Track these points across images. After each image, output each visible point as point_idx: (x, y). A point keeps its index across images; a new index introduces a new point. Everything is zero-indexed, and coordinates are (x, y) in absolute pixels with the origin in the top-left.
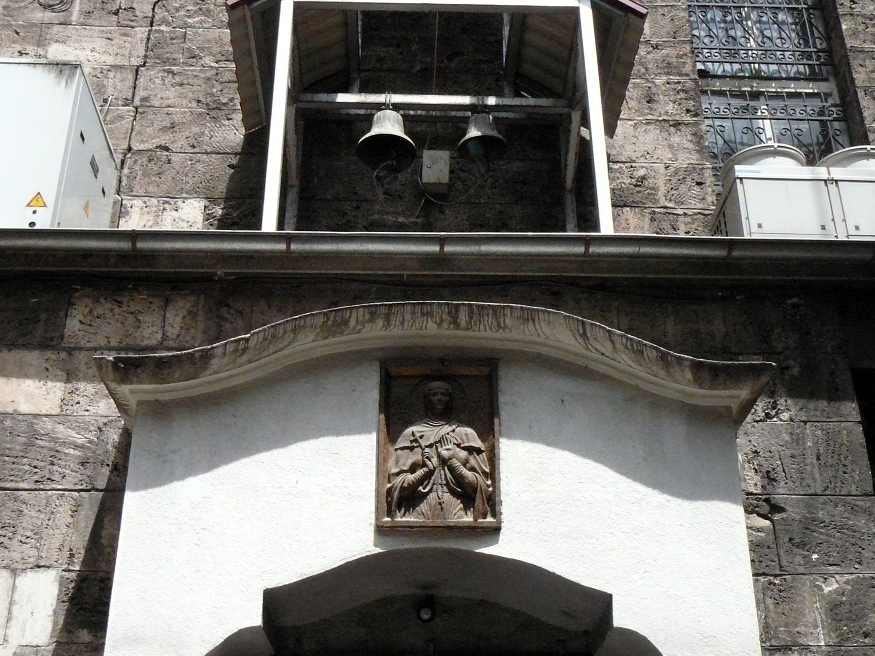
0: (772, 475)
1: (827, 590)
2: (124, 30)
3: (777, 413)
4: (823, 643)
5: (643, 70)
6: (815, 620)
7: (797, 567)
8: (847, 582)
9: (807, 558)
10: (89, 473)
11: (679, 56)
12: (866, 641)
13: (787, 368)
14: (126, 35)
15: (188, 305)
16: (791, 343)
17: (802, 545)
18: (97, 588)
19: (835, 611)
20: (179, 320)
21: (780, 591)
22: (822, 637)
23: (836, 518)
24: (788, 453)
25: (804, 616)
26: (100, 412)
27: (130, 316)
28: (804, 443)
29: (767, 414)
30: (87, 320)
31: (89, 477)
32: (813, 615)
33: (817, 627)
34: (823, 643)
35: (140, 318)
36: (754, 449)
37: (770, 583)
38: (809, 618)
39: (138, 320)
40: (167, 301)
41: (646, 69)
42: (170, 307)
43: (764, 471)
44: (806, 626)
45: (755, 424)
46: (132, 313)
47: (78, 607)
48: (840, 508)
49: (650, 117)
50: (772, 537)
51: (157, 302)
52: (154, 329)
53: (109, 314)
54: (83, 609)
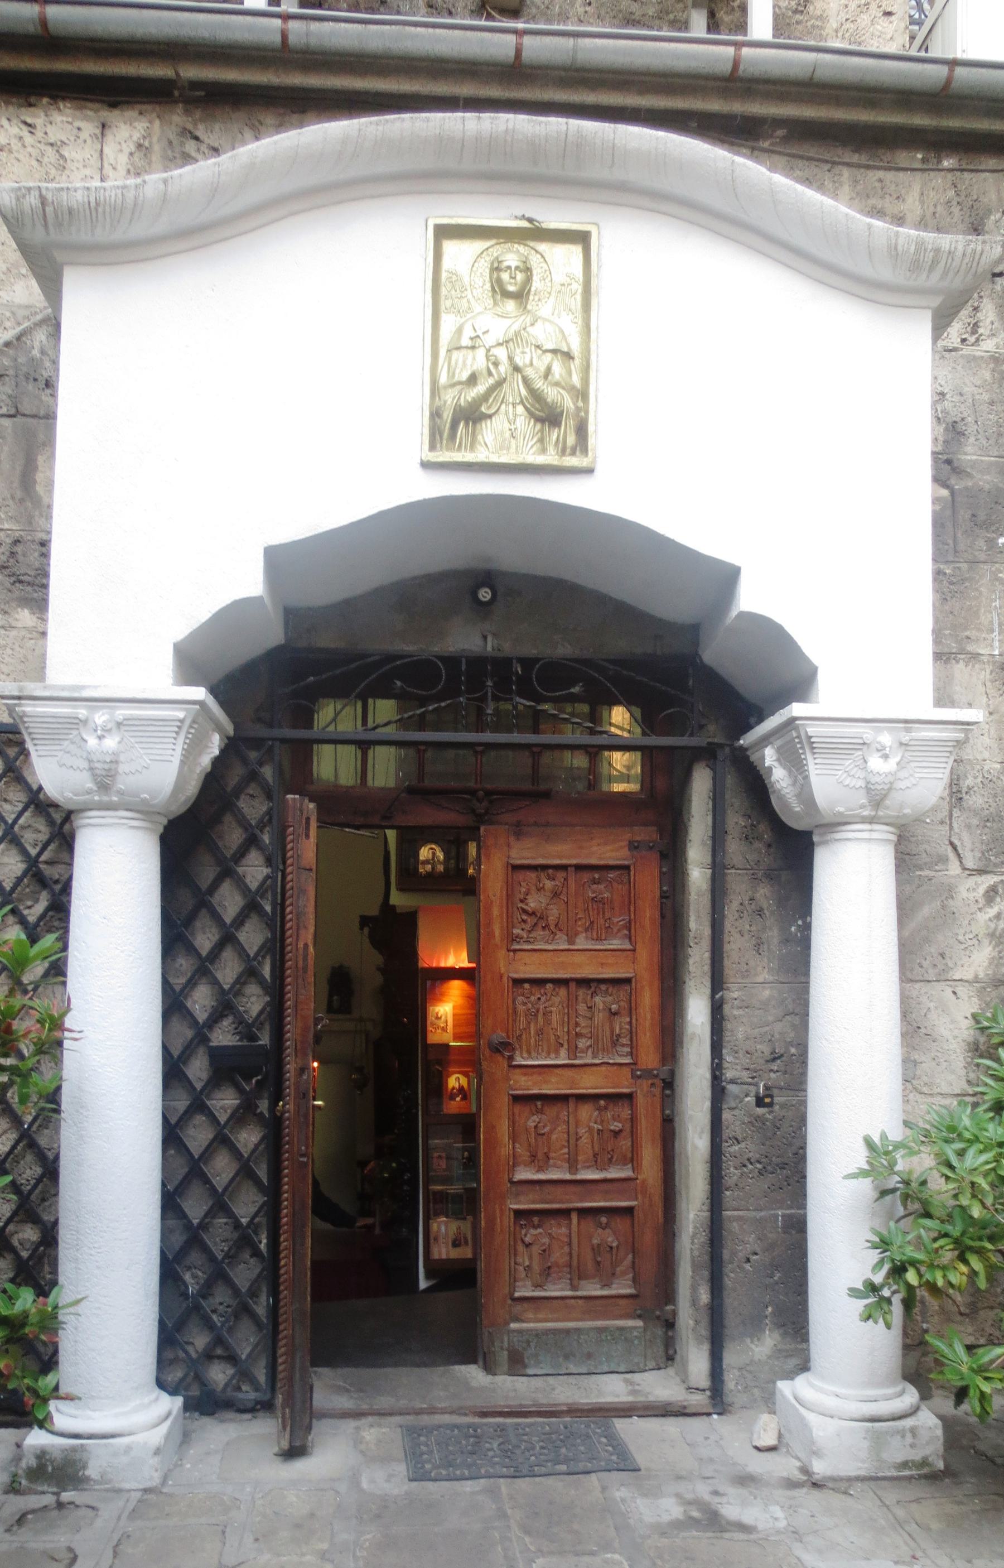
0: (960, 427)
3: (977, 340)
4: (996, 652)
6: (991, 622)
7: (977, 553)
10: (10, 392)
15: (136, 136)
17: (986, 525)
18: (36, 554)
20: (123, 159)
21: (952, 583)
22: (997, 644)
24: (986, 397)
25: (979, 618)
26: (17, 300)
27: (49, 149)
29: (964, 340)
31: (9, 396)
32: (989, 616)
33: (992, 631)
34: (996, 652)
35: (66, 154)
36: (940, 389)
38: (984, 619)
39: (62, 156)
40: (104, 126)
42: (109, 137)
43: (949, 420)
44: (979, 630)
45: (947, 355)
46: (52, 145)
47: (13, 579)
50: (948, 512)
51: (89, 128)
52: (88, 172)
53: (16, 145)
54: (21, 582)
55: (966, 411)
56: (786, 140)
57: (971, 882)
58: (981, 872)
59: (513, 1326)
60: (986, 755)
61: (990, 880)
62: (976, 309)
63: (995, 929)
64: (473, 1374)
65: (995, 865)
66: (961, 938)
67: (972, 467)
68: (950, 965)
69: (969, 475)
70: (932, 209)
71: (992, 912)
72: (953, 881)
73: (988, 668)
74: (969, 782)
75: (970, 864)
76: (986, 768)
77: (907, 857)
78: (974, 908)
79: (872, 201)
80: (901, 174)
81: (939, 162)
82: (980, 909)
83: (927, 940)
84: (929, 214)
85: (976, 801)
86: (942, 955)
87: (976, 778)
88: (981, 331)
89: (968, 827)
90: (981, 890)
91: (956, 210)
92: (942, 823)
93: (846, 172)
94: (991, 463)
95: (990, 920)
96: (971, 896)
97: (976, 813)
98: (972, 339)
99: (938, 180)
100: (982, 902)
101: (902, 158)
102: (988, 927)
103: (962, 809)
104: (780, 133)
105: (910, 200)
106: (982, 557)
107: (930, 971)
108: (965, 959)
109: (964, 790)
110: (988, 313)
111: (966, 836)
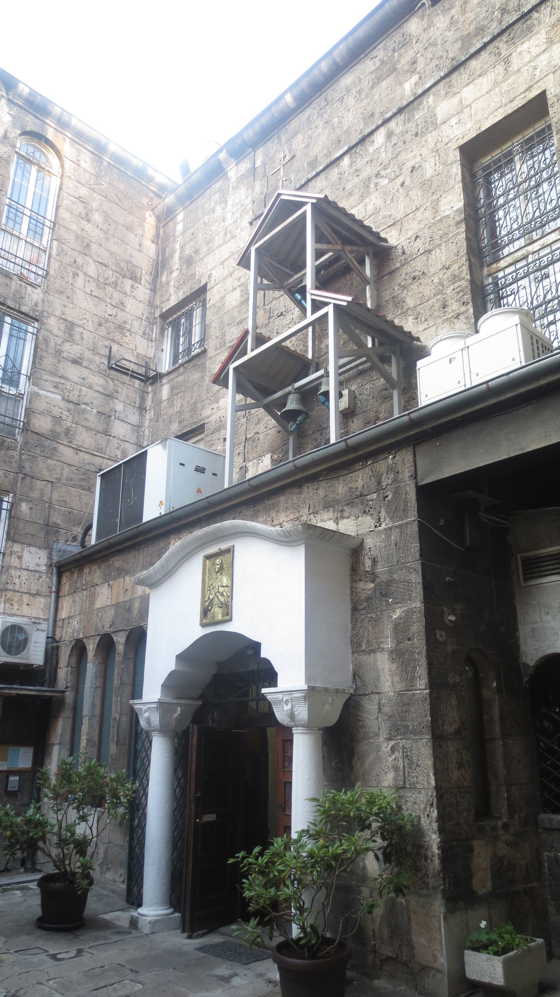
0: (376, 559)
5: (441, 288)
11: (460, 267)
16: (390, 481)
23: (402, 577)
24: (383, 545)
29: (376, 526)
37: (371, 617)
41: (443, 286)
49: (445, 318)
57: (386, 744)
60: (389, 689)
61: (392, 743)
62: (379, 512)
65: (394, 736)
71: (394, 757)
73: (387, 653)
78: (387, 755)
85: (386, 709)
86: (378, 775)
89: (384, 720)
91: (372, 478)
94: (385, 571)
99: (367, 470)
101: (357, 467)
106: (384, 608)
110: (383, 513)
111: (383, 724)
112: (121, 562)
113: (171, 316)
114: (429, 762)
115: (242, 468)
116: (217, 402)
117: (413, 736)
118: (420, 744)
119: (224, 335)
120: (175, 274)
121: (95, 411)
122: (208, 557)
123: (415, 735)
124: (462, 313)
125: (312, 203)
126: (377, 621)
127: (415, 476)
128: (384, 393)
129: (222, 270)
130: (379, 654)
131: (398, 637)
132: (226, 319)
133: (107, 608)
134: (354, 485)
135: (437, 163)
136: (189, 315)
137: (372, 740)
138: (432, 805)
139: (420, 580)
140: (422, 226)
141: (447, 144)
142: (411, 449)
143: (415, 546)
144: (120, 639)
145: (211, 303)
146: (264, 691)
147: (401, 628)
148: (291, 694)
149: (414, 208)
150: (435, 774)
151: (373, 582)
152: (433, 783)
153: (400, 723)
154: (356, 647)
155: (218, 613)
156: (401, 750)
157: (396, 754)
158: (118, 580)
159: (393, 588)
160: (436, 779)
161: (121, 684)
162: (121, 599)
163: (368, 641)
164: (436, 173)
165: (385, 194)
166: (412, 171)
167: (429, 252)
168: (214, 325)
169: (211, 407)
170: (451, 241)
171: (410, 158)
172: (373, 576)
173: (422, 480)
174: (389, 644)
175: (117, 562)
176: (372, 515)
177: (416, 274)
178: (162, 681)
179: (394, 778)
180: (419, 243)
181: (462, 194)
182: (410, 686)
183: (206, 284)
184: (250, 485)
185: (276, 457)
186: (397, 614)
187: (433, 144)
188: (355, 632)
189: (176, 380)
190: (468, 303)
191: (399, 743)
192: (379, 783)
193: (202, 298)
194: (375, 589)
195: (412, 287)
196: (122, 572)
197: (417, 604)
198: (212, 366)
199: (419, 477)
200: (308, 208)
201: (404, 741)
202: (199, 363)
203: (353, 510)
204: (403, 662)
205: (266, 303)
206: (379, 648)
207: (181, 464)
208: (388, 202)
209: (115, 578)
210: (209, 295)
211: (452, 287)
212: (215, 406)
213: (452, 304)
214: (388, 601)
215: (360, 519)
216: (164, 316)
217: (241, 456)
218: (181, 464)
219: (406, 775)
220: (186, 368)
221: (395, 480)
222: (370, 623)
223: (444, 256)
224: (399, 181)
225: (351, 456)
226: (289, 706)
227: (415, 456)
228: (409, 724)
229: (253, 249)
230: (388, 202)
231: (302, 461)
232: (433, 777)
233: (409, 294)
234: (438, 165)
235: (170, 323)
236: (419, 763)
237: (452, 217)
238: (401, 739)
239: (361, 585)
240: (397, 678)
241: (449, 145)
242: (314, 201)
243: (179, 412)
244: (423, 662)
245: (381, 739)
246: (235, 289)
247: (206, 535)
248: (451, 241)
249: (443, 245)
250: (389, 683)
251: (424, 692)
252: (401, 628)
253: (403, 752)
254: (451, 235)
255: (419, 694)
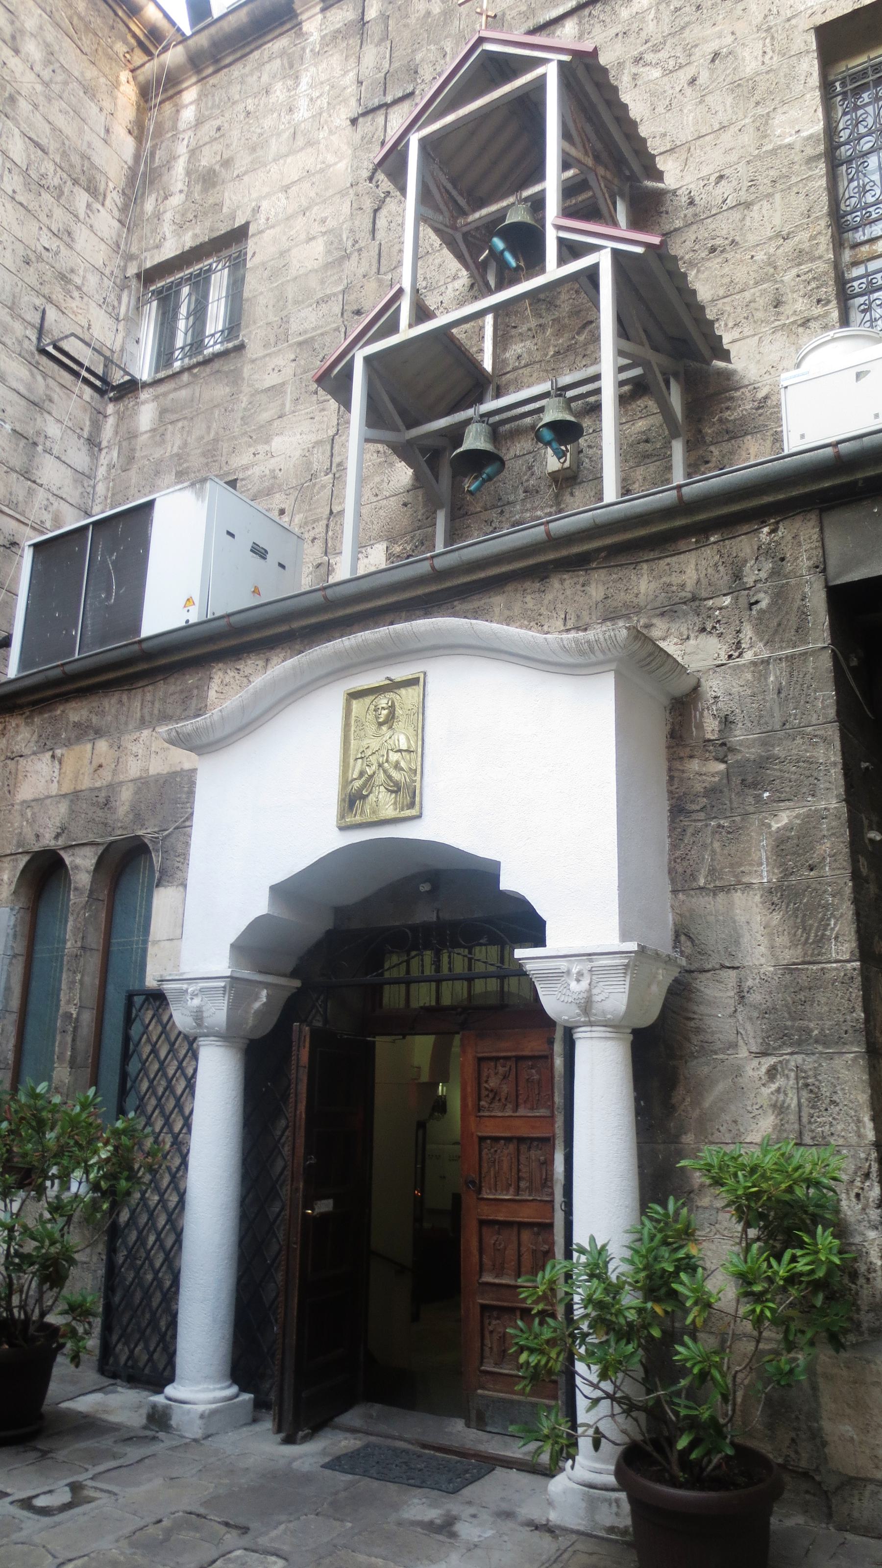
0: (731, 718)
1: (775, 826)
2: (321, 406)
5: (772, 270)
8: (796, 817)
9: (758, 798)
11: (813, 238)
12: (812, 873)
13: (757, 602)
14: (323, 410)
16: (763, 575)
17: (755, 785)
19: (782, 847)
21: (729, 833)
22: (765, 874)
24: (749, 692)
25: (750, 855)
28: (766, 679)
29: (730, 656)
30: (219, 690)
33: (762, 864)
41: (775, 268)
43: (722, 715)
44: (750, 865)
45: (718, 669)
48: (799, 741)
49: (777, 323)
50: (725, 781)
55: (734, 706)
56: (606, 558)
57: (755, 1063)
58: (764, 1054)
59: (480, 1391)
60: (763, 960)
62: (738, 632)
63: (777, 1101)
64: (458, 1425)
65: (775, 1049)
66: (749, 1108)
67: (740, 745)
68: (742, 1130)
69: (739, 751)
70: (704, 572)
71: (774, 1087)
72: (740, 1062)
74: (750, 983)
75: (754, 1049)
76: (762, 971)
77: (705, 1045)
78: (758, 1084)
79: (664, 579)
80: (682, 556)
81: (708, 539)
82: (764, 1085)
83: (722, 1110)
84: (702, 576)
85: (756, 998)
86: (735, 1122)
87: (754, 979)
88: (743, 646)
89: (750, 1019)
90: (764, 1069)
91: (721, 568)
92: (730, 1016)
93: (645, 566)
94: (755, 740)
95: (772, 1093)
96: (756, 1074)
97: (755, 1007)
98: (737, 654)
99: (708, 552)
100: (765, 1078)
101: (682, 545)
102: (770, 1099)
103: (744, 1005)
104: (603, 554)
105: (688, 571)
106: (751, 809)
107: (727, 1135)
108: (754, 1126)
109: (746, 989)
110: (748, 632)
111: (749, 1026)
112: (85, 713)
113: (162, 277)
114: (863, 1097)
115: (318, 566)
116: (267, 441)
117: (820, 1048)
118: (838, 1062)
119: (285, 320)
120: (176, 200)
121: (8, 427)
122: (355, 695)
123: (825, 1044)
124: (816, 319)
125: (561, 63)
126: (734, 833)
127: (821, 568)
128: (642, 446)
129: (284, 201)
130: (739, 893)
131: (785, 864)
132: (291, 292)
133: (48, 801)
134: (675, 579)
135: (768, 50)
136: (201, 283)
137: (721, 1056)
138: (867, 1176)
139: (839, 759)
140: (733, 157)
141: (789, 20)
142: (813, 517)
143: (825, 699)
144: (82, 864)
145: (257, 260)
146: (519, 953)
147: (787, 848)
148: (591, 961)
149: (717, 126)
150: (874, 1119)
151: (723, 761)
152: (870, 1135)
153: (789, 1023)
154: (682, 879)
155: (384, 803)
156: (792, 1075)
157: (780, 1082)
158: (77, 748)
159: (773, 772)
160: (876, 1129)
161: (83, 948)
162: (86, 783)
163: (712, 871)
164: (765, 68)
165: (653, 94)
166: (713, 61)
167: (748, 205)
168: (262, 300)
169: (252, 450)
170: (795, 190)
171: (711, 36)
172: (723, 749)
173: (839, 575)
174: (764, 874)
175: (76, 712)
176: (720, 635)
177: (718, 242)
178: (233, 937)
179: (775, 1127)
180: (725, 188)
181: (820, 110)
182: (812, 955)
183: (247, 224)
184: (433, 567)
185: (397, 549)
186: (782, 820)
187: (760, 18)
188: (678, 853)
189: (171, 396)
190: (828, 302)
191: (788, 1061)
192: (739, 1134)
193: (233, 250)
194: (728, 775)
195: (708, 264)
196: (87, 732)
197: (830, 800)
198: (256, 376)
199: (831, 570)
200: (551, 73)
201: (799, 1058)
202: (226, 368)
203: (674, 627)
204: (797, 909)
205: (383, 270)
206: (739, 883)
207: (229, 533)
208: (660, 109)
209: (68, 743)
210: (251, 245)
211: (794, 271)
212: (261, 448)
213: (795, 301)
214: (760, 796)
215: (692, 642)
216: (148, 276)
217: (319, 544)
218: (229, 533)
219: (805, 1120)
220: (195, 375)
221: (775, 573)
222: (717, 836)
223: (778, 214)
224: (683, 76)
225: (679, 522)
226: (584, 984)
227: (822, 530)
228: (812, 1025)
229: (414, 140)
230: (660, 109)
231: (451, 560)
232: (870, 1125)
233: (701, 276)
234: (770, 54)
235: (153, 292)
236: (835, 1098)
237: (798, 147)
238: (792, 1054)
239: (695, 765)
240: (782, 940)
241: (793, 22)
242: (566, 58)
243: (177, 455)
244: (847, 909)
245: (743, 1053)
246: (314, 238)
247: (359, 649)
248: (795, 190)
249: (778, 196)
250: (762, 949)
251: (849, 966)
252: (787, 848)
253: (797, 1078)
254: (794, 179)
255: (836, 969)
